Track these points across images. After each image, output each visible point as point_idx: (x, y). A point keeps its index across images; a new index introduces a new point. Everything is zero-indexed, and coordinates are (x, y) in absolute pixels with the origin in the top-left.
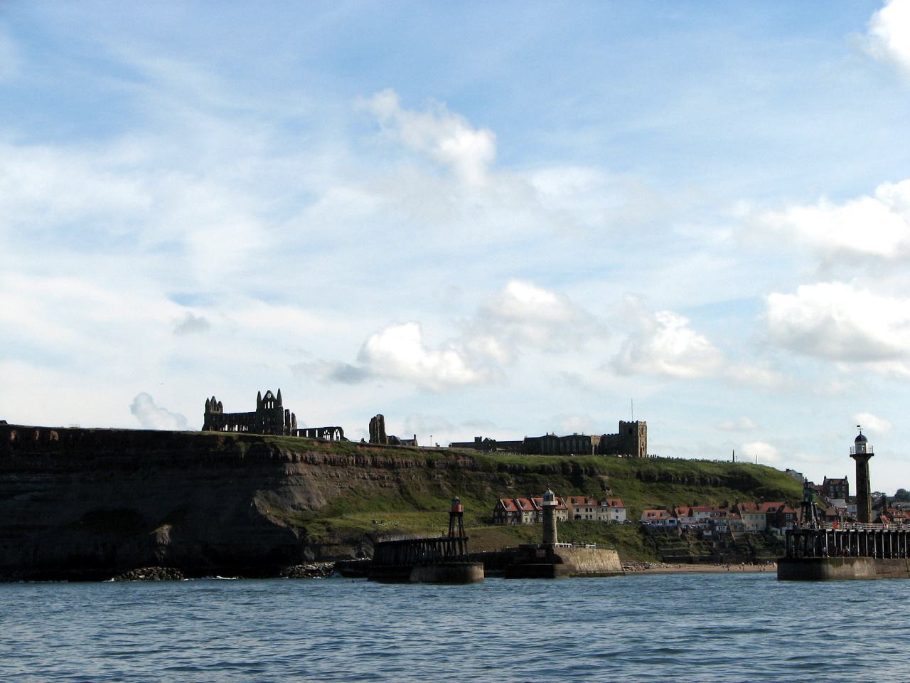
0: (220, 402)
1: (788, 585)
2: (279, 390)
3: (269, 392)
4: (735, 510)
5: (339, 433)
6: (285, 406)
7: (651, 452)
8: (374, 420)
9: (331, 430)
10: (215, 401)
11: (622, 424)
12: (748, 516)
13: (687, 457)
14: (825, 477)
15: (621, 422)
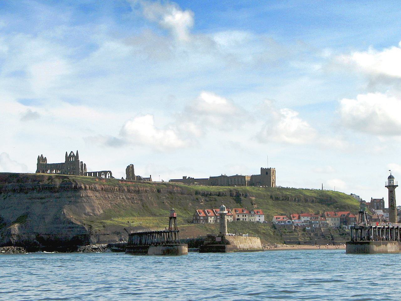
0: (45, 157)
1: (352, 256)
2: (77, 151)
3: (72, 152)
4: (323, 216)
5: (109, 174)
6: (80, 159)
7: (278, 184)
8: (128, 167)
9: (105, 173)
10: (43, 157)
11: (262, 170)
12: (330, 219)
13: (297, 187)
14: (372, 198)
15: (261, 168)
